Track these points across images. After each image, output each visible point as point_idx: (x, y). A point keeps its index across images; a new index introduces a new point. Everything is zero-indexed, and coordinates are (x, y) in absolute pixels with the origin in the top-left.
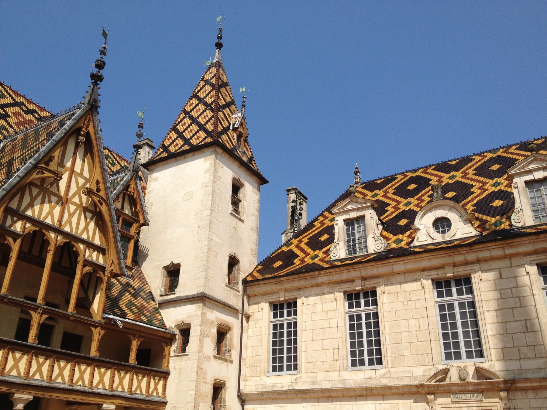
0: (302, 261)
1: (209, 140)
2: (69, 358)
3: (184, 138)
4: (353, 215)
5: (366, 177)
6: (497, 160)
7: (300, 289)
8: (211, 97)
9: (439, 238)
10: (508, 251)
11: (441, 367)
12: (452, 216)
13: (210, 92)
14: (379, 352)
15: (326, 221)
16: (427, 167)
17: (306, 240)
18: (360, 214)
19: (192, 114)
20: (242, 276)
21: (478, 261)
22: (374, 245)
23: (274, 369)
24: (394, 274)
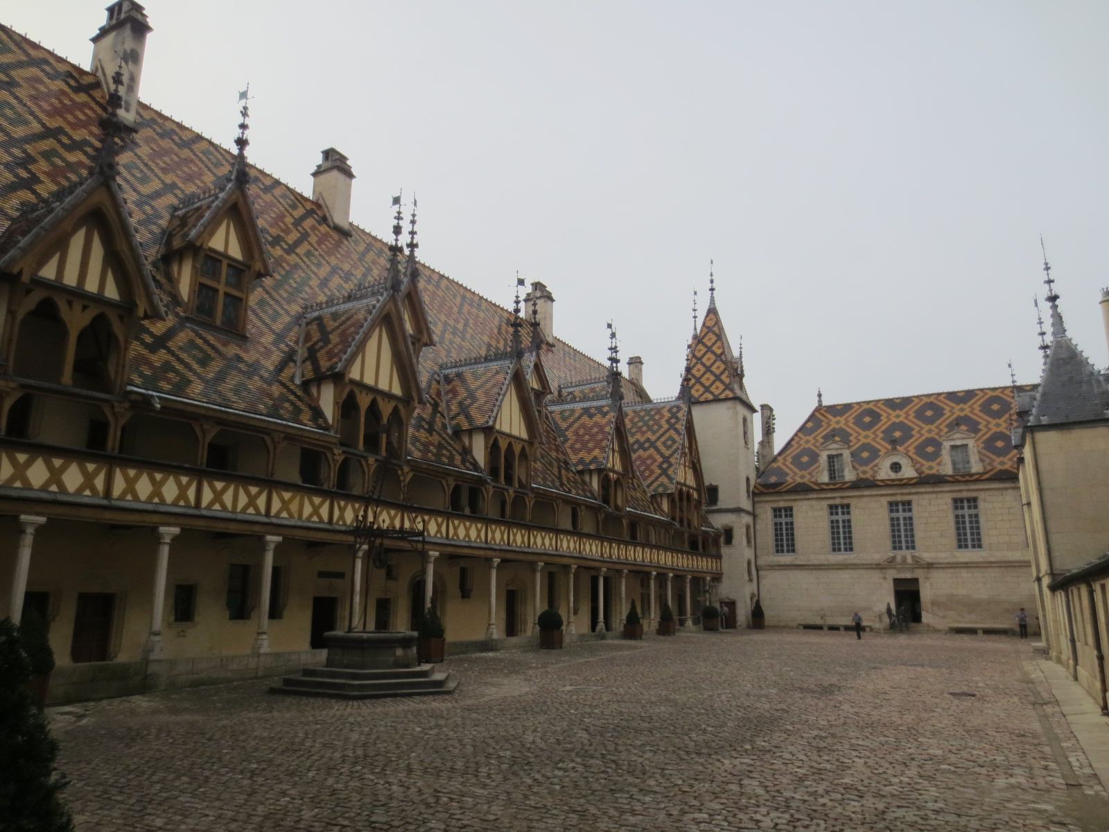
0: (792, 478)
1: (729, 394)
2: (692, 554)
3: (703, 385)
4: (834, 453)
5: (826, 403)
6: (930, 406)
7: (795, 500)
8: (719, 348)
9: (893, 476)
10: (936, 490)
11: (891, 554)
12: (904, 462)
13: (716, 342)
14: (851, 543)
15: (802, 442)
16: (878, 401)
17: (789, 459)
18: (839, 452)
19: (704, 360)
20: (751, 489)
21: (917, 493)
22: (849, 475)
23: (777, 551)
24: (863, 496)
